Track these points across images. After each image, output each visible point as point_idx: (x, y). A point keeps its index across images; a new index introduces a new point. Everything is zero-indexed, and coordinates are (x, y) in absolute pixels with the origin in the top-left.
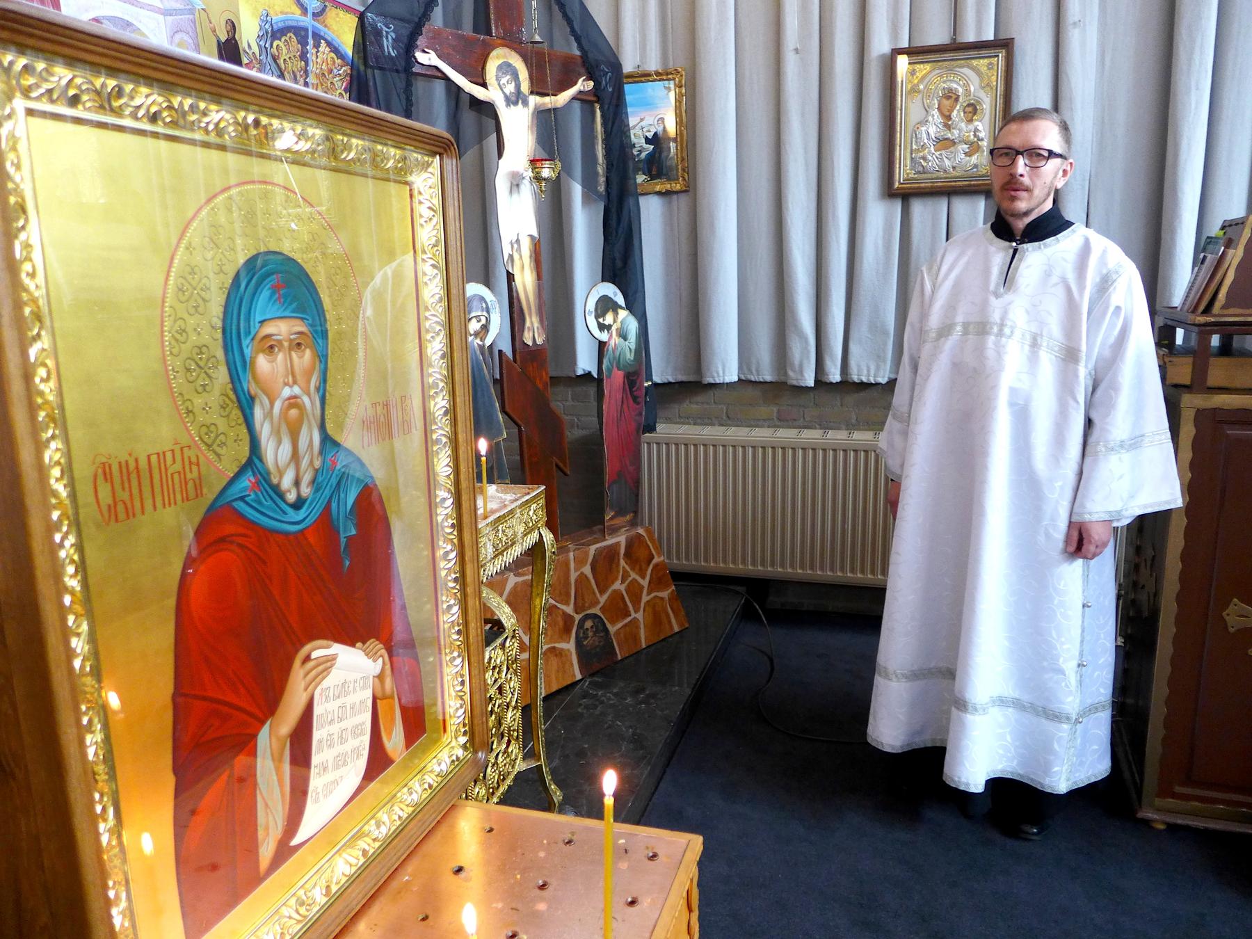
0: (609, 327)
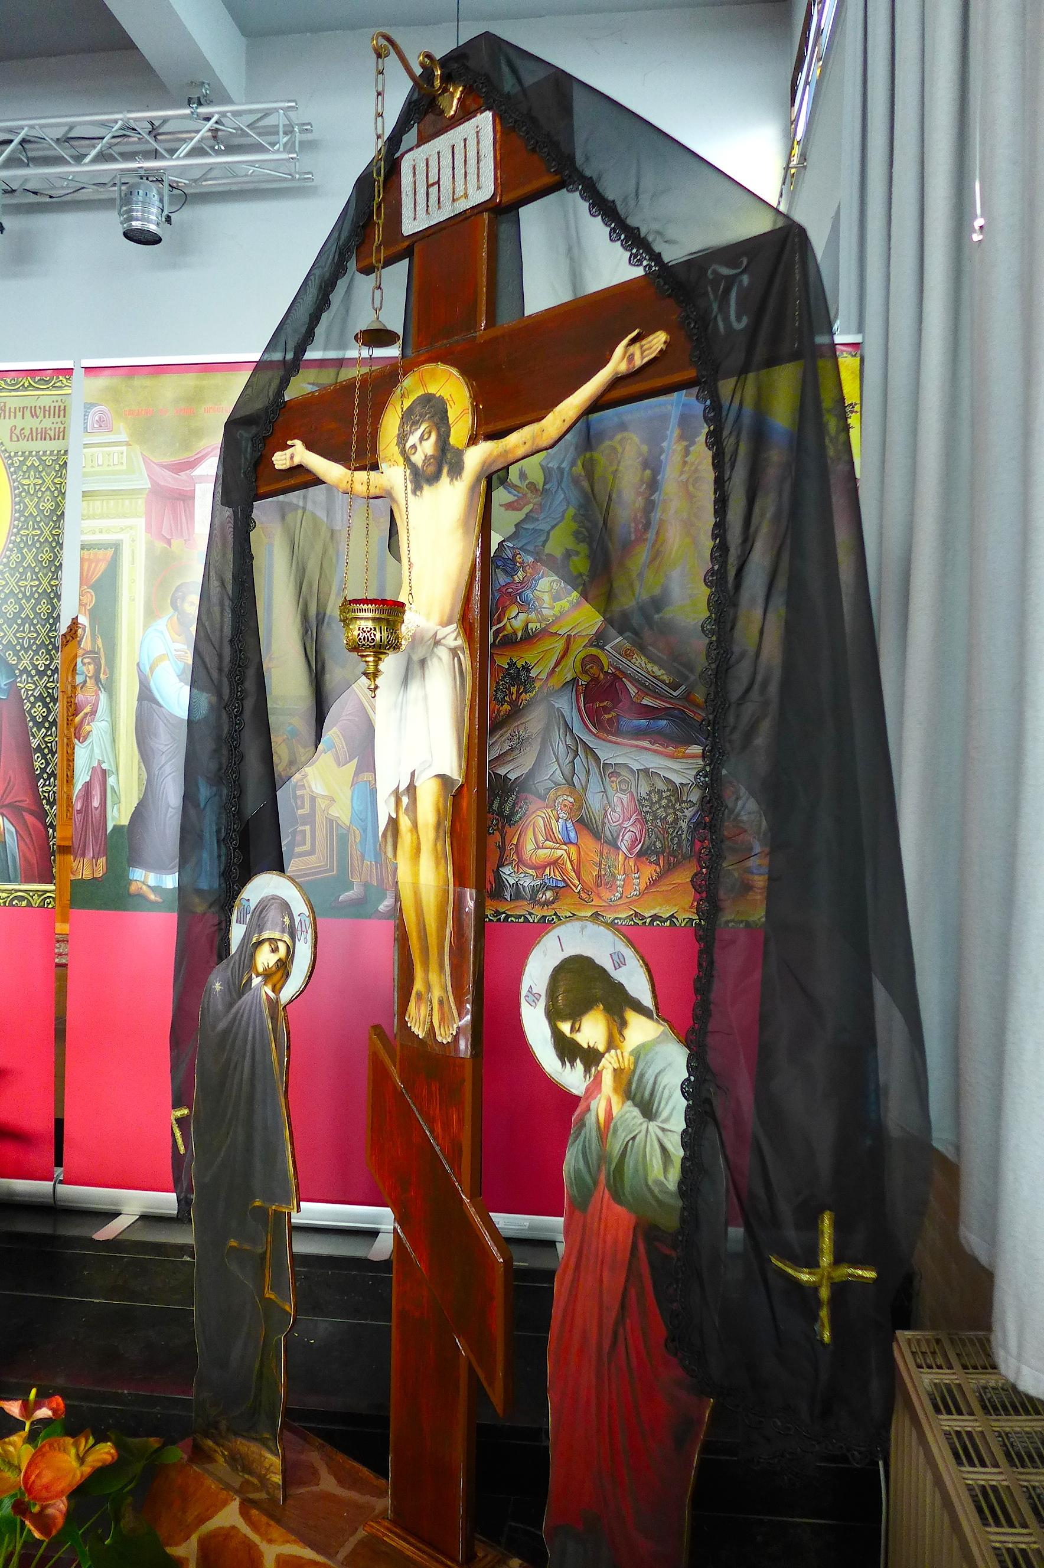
0: (591, 1058)
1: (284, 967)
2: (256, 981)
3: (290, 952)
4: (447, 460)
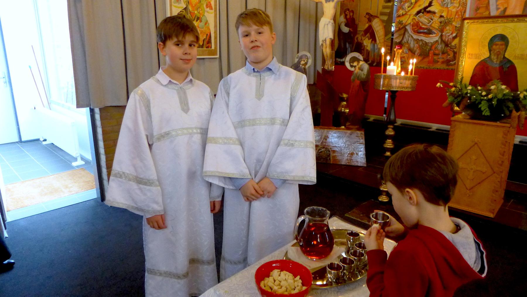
0: (355, 67)
1: (306, 64)
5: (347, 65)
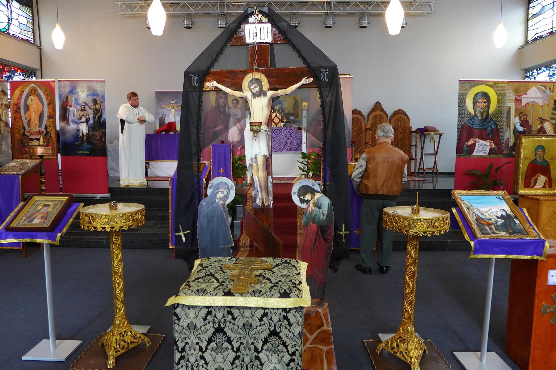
0: (308, 202)
1: (227, 197)
2: (217, 201)
3: (228, 193)
4: (261, 93)
5: (295, 199)
